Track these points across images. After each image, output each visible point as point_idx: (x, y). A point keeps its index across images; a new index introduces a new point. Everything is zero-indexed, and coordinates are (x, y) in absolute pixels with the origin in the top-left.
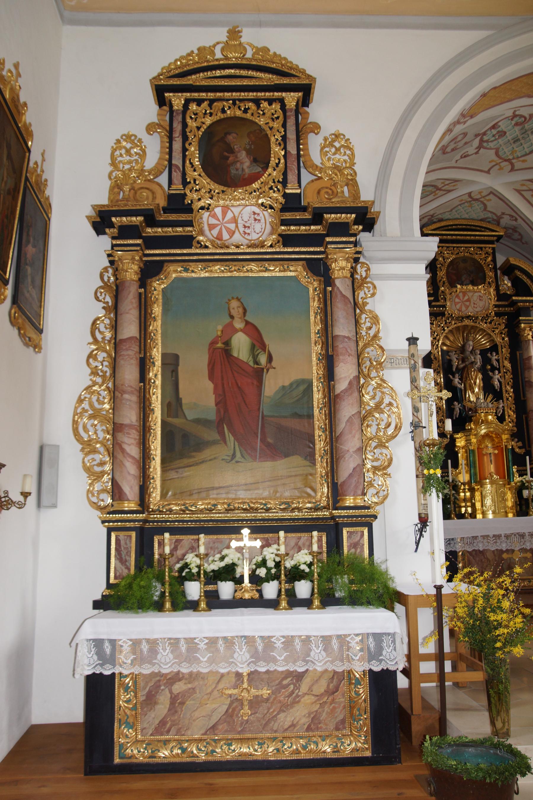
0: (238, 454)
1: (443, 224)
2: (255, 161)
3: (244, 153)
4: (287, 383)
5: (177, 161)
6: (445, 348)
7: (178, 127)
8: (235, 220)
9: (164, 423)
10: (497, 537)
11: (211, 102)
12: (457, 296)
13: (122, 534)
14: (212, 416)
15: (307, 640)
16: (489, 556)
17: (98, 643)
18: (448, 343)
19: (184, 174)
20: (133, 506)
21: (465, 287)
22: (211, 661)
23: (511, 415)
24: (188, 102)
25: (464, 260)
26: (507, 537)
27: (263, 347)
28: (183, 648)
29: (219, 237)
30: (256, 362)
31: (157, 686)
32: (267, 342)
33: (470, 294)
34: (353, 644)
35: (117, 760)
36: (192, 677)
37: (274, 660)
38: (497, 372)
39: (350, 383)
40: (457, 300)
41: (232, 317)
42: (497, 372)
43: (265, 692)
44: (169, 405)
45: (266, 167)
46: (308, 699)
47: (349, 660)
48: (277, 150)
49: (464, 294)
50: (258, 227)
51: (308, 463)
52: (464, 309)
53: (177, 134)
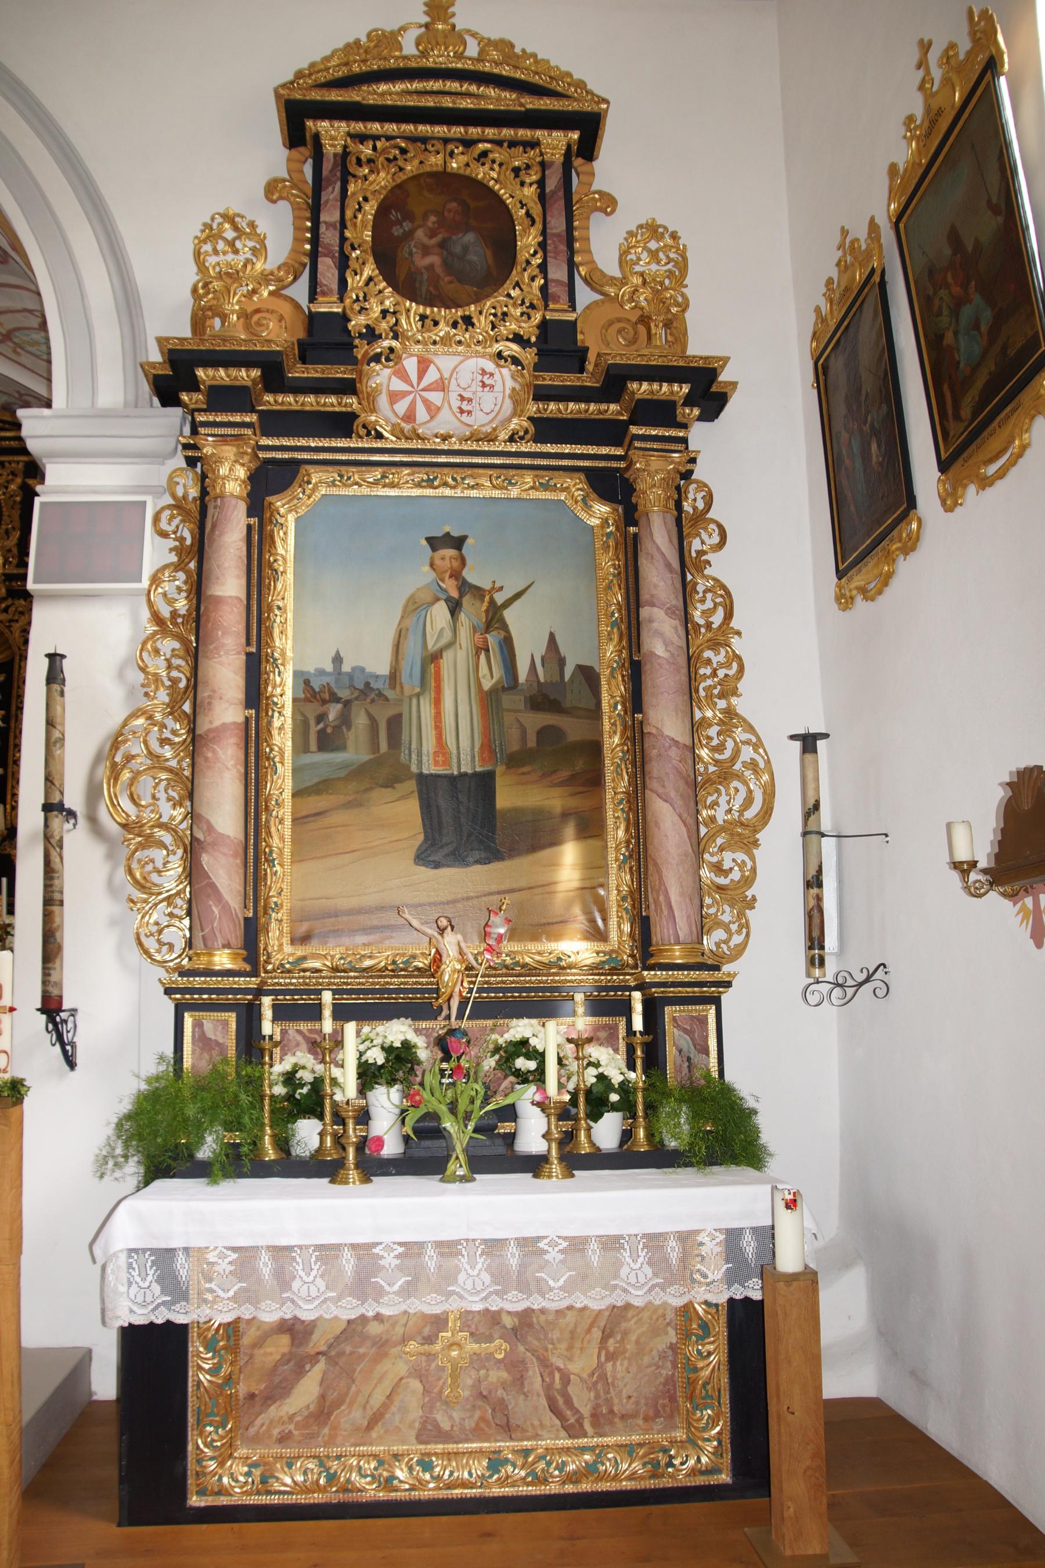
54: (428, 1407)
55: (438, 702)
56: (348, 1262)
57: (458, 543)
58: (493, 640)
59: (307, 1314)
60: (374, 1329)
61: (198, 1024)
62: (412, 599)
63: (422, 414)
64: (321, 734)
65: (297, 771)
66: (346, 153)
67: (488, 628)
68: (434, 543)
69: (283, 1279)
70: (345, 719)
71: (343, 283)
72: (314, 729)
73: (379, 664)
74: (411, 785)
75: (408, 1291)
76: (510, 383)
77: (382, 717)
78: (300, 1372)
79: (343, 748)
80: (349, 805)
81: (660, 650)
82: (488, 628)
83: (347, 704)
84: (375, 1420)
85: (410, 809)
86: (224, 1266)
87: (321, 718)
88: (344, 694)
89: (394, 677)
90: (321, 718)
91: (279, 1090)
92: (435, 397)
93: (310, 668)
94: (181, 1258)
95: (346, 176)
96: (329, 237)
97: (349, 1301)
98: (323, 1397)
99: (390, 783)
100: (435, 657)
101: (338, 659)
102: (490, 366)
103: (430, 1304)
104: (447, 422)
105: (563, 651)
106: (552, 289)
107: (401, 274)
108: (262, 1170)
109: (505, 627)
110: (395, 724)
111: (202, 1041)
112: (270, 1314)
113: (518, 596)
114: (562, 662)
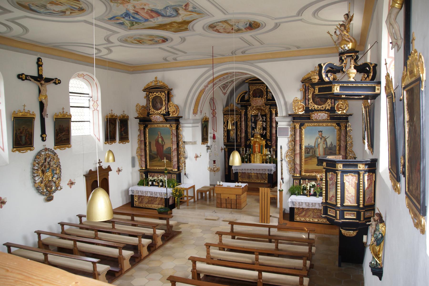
0: (160, 160)
1: (251, 79)
2: (161, 105)
3: (159, 103)
4: (167, 148)
5: (148, 106)
6: (253, 114)
7: (148, 98)
8: (157, 118)
9: (149, 154)
10: (248, 169)
11: (153, 93)
12: (254, 101)
13: (142, 173)
14: (156, 153)
15: (157, 193)
16: (247, 174)
17: (132, 190)
18: (253, 112)
19: (149, 108)
20: (144, 168)
21: (256, 98)
22: (145, 194)
23: (268, 134)
24: (149, 93)
25: (258, 89)
26: (250, 170)
27: (164, 141)
28: (142, 192)
29: (155, 120)
30: (163, 144)
31: (140, 197)
32: (164, 140)
33: (257, 100)
34: (163, 194)
35: (135, 206)
36: (143, 196)
37: (153, 195)
38: (264, 122)
39: (174, 150)
40: (254, 102)
41: (159, 135)
42: (264, 122)
43: (153, 199)
44: (150, 151)
45: (162, 107)
46: (158, 201)
47: (162, 196)
48: (164, 103)
49: (256, 100)
50: (161, 119)
51: (170, 162)
52: (256, 104)
53: (148, 100)
54: (313, 215)
55: (319, 149)
56: (307, 204)
57: (321, 132)
58: (325, 142)
59: (304, 207)
60: (309, 209)
61: (295, 181)
62: (317, 138)
63: (317, 118)
64: (307, 152)
65: (305, 156)
66: (309, 86)
67: (325, 141)
68: (319, 132)
69: (302, 205)
70: (310, 151)
71: (309, 103)
72: (306, 152)
73: (313, 145)
74: (316, 158)
75: (312, 206)
76: (327, 115)
77: (313, 150)
78: (303, 212)
79: (309, 154)
80: (310, 159)
81: (342, 145)
82: (325, 141)
83: (310, 149)
84: (309, 216)
85: (316, 160)
86: (297, 203)
87: (307, 151)
88: (309, 148)
89: (315, 146)
90: (307, 151)
91: (302, 188)
92: (319, 117)
93: (306, 145)
94: (294, 203)
95: (309, 89)
96: (307, 97)
97: (307, 207)
98: (305, 214)
99: (314, 157)
100: (319, 144)
101: (309, 144)
102: (324, 114)
103: (314, 208)
104: (320, 119)
105: (333, 144)
106: (332, 103)
107: (315, 101)
108: (301, 195)
109: (326, 141)
110: (315, 151)
111: (296, 183)
112: (301, 207)
113: (328, 137)
114: (332, 145)
